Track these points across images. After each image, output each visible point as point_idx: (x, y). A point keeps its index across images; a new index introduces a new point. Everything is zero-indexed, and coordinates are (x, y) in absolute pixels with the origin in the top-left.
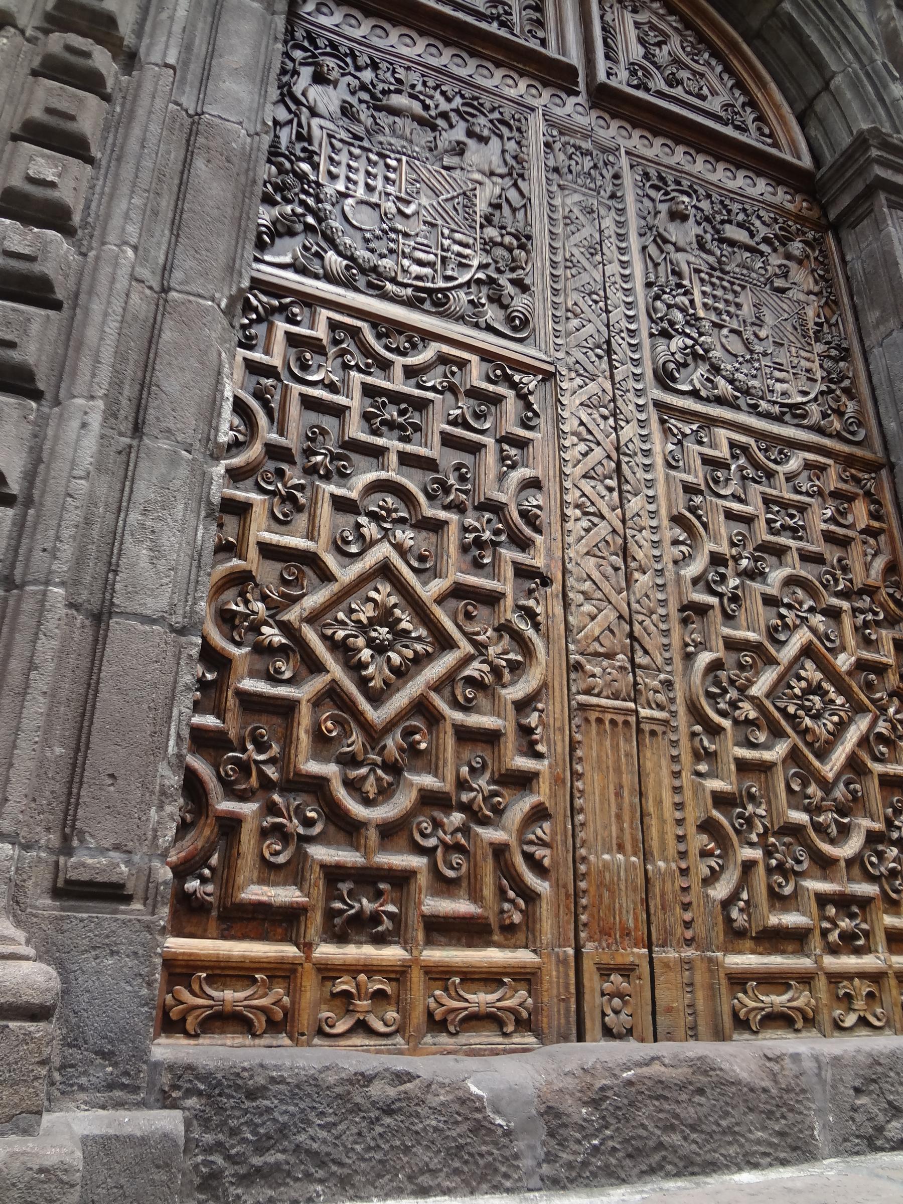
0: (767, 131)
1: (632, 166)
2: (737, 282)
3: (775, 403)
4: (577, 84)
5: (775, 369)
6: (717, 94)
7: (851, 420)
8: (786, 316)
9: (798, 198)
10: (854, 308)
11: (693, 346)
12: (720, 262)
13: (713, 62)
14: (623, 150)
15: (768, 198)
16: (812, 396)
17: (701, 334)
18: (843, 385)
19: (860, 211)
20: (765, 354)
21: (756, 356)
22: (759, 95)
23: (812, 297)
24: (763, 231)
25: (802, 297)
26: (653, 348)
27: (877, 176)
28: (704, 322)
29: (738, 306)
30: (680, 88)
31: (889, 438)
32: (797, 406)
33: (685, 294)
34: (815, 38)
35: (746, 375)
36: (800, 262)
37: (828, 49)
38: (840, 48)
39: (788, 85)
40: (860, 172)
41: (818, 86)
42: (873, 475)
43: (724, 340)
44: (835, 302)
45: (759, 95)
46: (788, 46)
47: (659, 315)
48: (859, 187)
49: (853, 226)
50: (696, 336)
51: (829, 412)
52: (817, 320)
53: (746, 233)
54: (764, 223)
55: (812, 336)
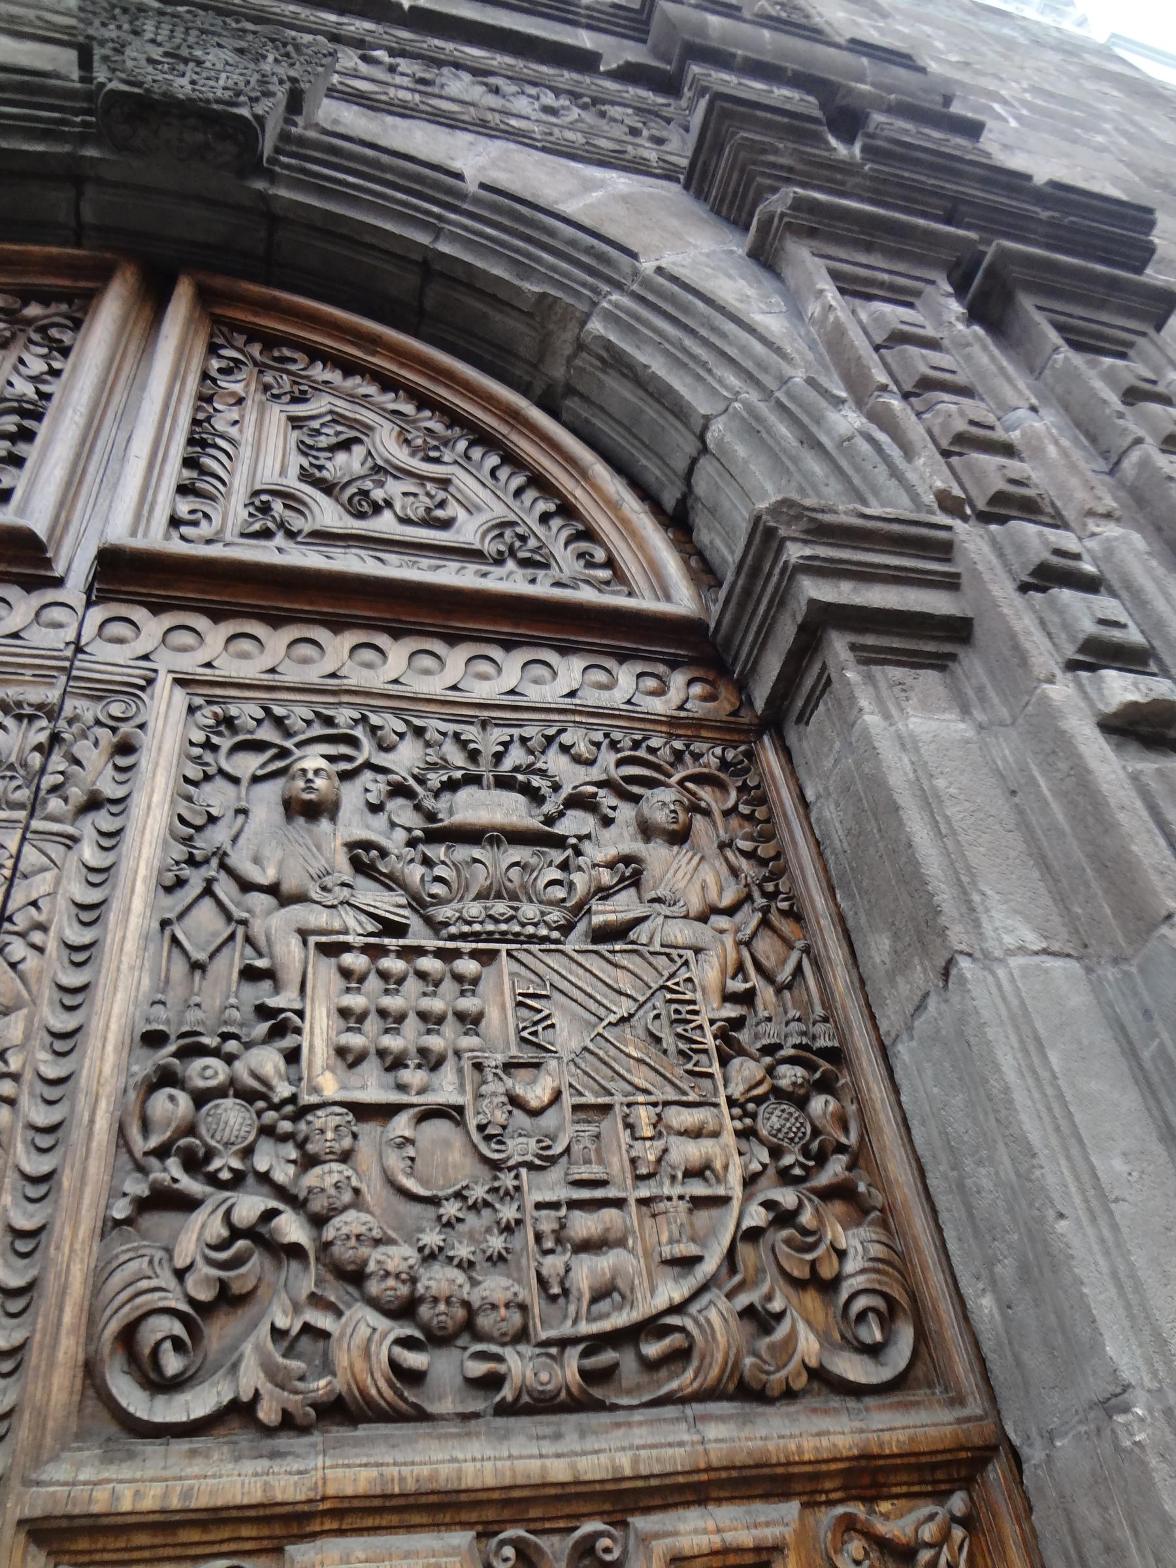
0: (600, 555)
1: (191, 710)
2: (466, 946)
3: (563, 1343)
4: (48, 563)
5: (573, 1204)
6: (479, 509)
7: (861, 1303)
8: (624, 1007)
9: (678, 680)
10: (841, 919)
11: (269, 1215)
12: (418, 903)
13: (477, 453)
14: (164, 681)
15: (591, 698)
16: (710, 1265)
17: (309, 1161)
18: (824, 1178)
19: (809, 683)
20: (544, 1162)
21: (507, 1180)
22: (578, 492)
23: (721, 922)
24: (572, 777)
25: (681, 932)
26: (100, 1276)
27: (812, 602)
28: (320, 1119)
29: (471, 1021)
30: (387, 515)
31: (986, 1349)
32: (652, 1327)
33: (280, 1030)
34: (658, 366)
35: (467, 1266)
36: (679, 837)
37: (689, 380)
38: (709, 371)
39: (644, 462)
40: (780, 600)
41: (690, 447)
42: (958, 1503)
43: (395, 1161)
44: (795, 915)
45: (578, 492)
46: (618, 389)
47: (154, 1142)
48: (786, 632)
49: (803, 718)
50: (283, 1174)
51: (776, 1306)
52: (738, 986)
53: (516, 800)
54: (578, 760)
55: (710, 1042)
